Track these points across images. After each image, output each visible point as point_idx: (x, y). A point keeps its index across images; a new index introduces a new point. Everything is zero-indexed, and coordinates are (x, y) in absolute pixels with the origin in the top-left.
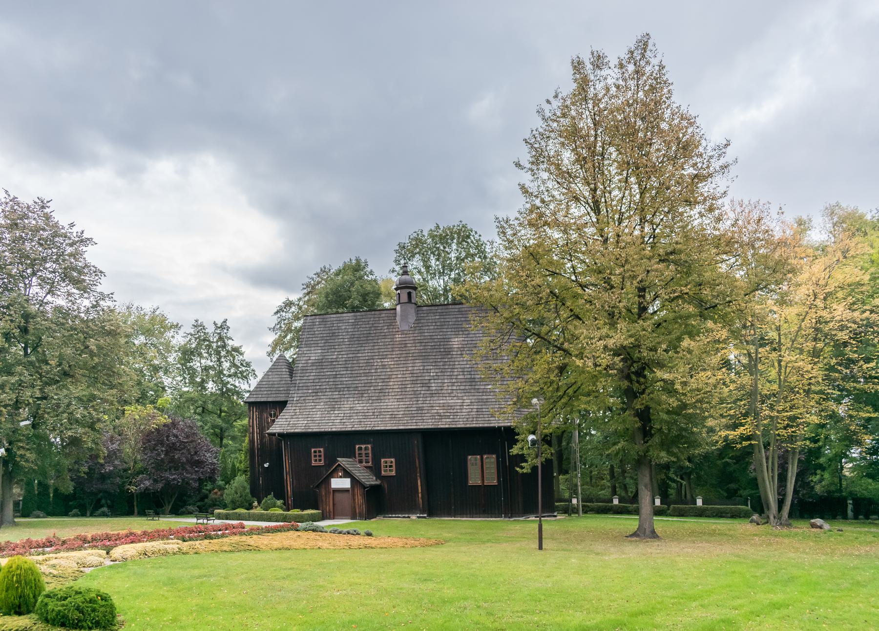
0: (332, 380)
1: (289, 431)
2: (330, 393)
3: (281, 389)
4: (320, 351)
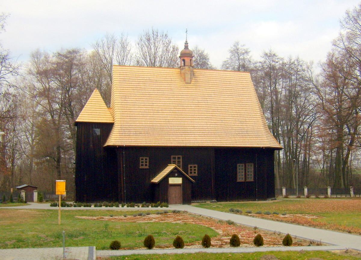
1: (126, 144)
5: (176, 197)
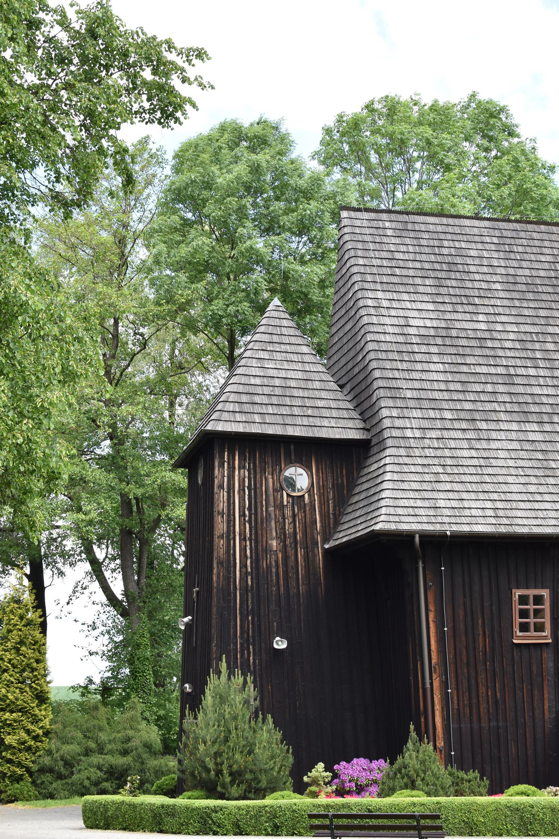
0: (501, 389)
1: (455, 528)
2: (515, 426)
3: (320, 403)
4: (431, 307)
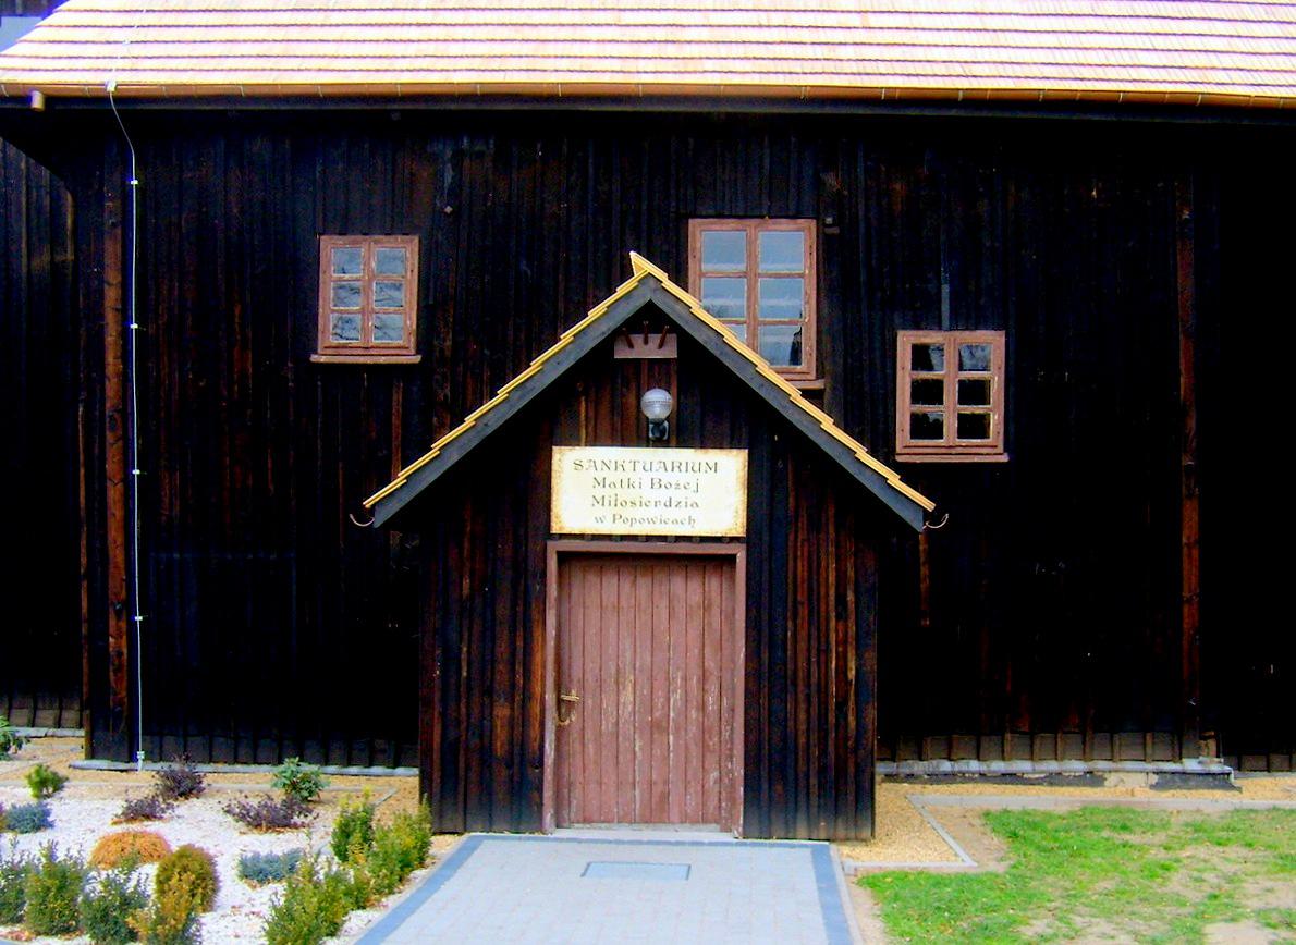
5: (657, 728)
